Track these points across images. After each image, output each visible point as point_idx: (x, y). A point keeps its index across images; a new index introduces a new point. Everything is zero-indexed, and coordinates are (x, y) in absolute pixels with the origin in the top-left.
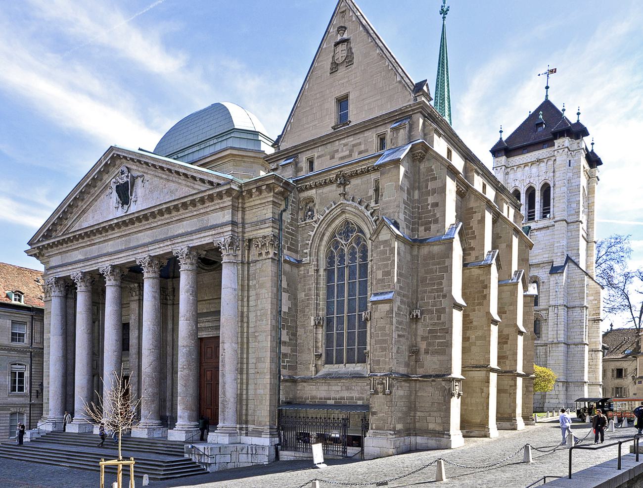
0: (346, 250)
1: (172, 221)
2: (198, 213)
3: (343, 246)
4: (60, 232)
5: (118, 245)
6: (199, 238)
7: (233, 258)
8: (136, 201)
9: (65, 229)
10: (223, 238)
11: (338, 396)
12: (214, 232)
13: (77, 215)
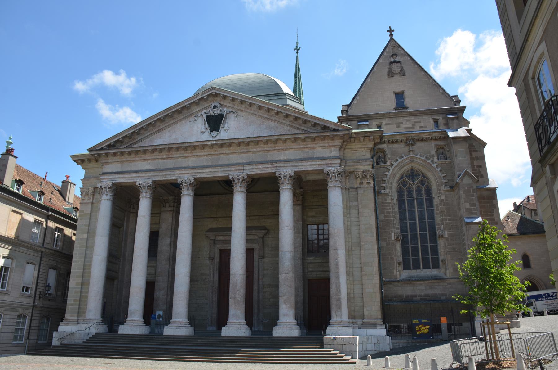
0: (414, 188)
1: (274, 150)
2: (305, 146)
3: (412, 185)
4: (126, 144)
5: (204, 161)
6: (305, 165)
7: (339, 183)
8: (228, 130)
9: (133, 142)
10: (334, 168)
11: (422, 294)
12: (321, 163)
13: (151, 132)
